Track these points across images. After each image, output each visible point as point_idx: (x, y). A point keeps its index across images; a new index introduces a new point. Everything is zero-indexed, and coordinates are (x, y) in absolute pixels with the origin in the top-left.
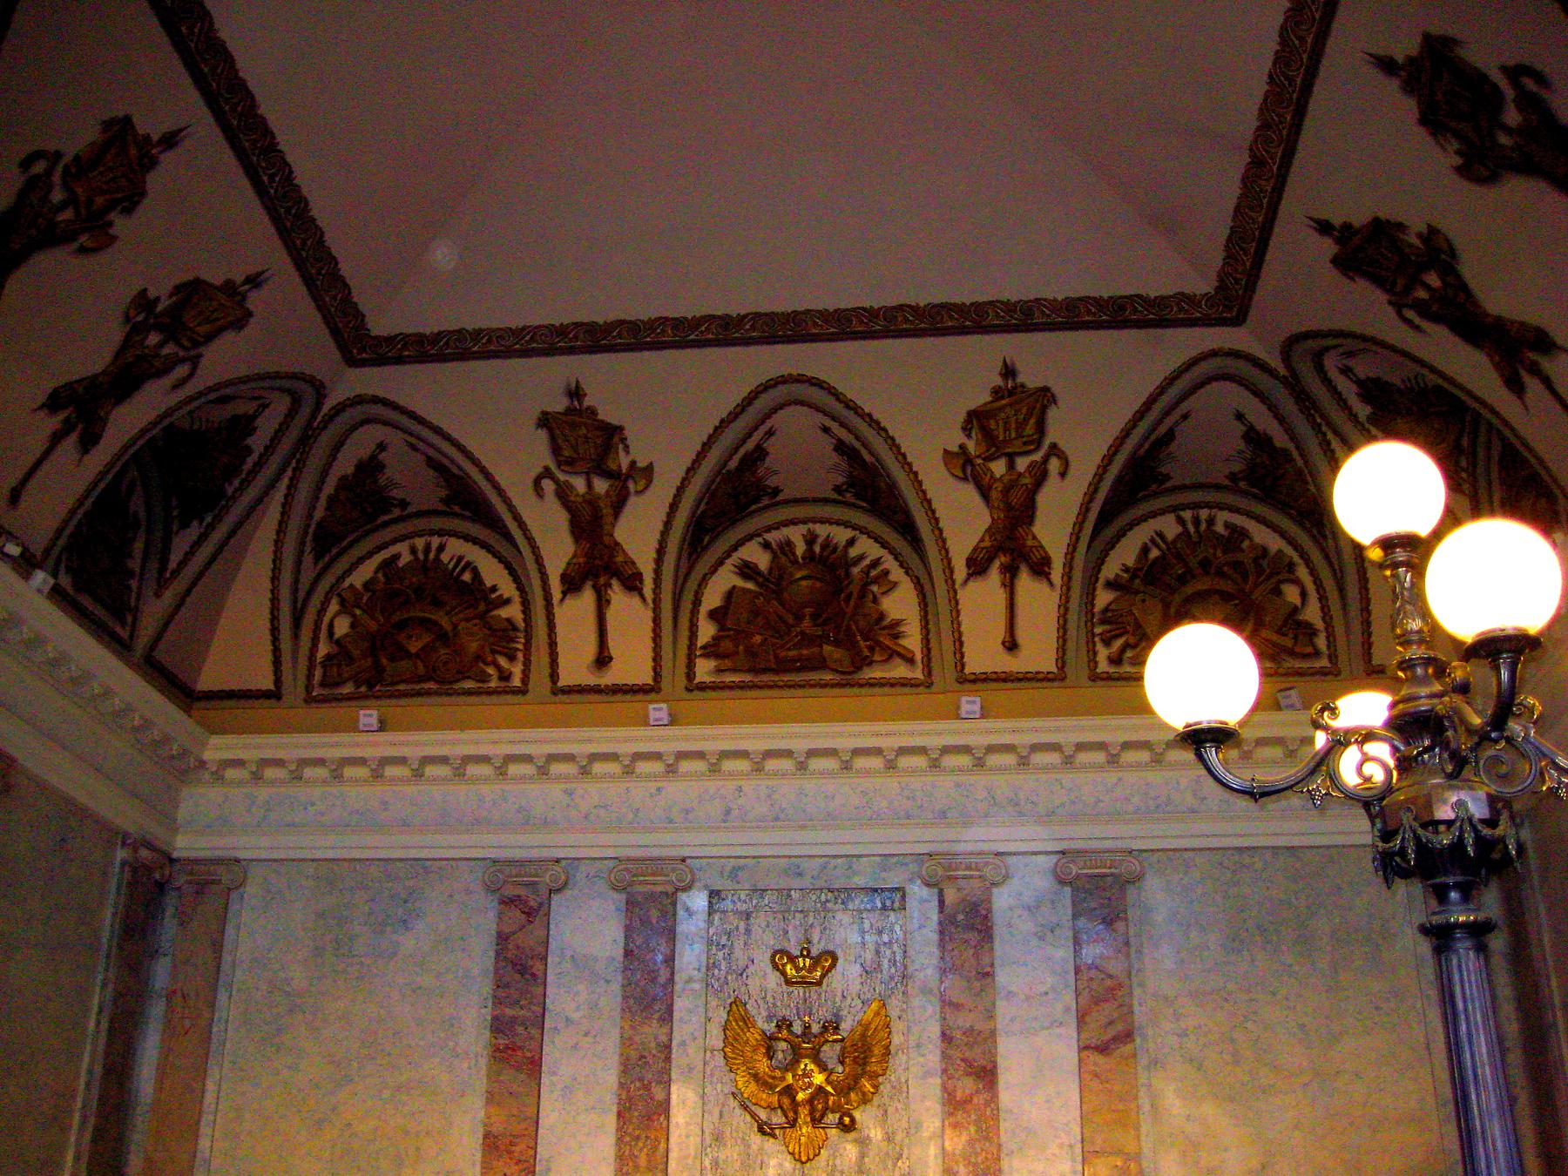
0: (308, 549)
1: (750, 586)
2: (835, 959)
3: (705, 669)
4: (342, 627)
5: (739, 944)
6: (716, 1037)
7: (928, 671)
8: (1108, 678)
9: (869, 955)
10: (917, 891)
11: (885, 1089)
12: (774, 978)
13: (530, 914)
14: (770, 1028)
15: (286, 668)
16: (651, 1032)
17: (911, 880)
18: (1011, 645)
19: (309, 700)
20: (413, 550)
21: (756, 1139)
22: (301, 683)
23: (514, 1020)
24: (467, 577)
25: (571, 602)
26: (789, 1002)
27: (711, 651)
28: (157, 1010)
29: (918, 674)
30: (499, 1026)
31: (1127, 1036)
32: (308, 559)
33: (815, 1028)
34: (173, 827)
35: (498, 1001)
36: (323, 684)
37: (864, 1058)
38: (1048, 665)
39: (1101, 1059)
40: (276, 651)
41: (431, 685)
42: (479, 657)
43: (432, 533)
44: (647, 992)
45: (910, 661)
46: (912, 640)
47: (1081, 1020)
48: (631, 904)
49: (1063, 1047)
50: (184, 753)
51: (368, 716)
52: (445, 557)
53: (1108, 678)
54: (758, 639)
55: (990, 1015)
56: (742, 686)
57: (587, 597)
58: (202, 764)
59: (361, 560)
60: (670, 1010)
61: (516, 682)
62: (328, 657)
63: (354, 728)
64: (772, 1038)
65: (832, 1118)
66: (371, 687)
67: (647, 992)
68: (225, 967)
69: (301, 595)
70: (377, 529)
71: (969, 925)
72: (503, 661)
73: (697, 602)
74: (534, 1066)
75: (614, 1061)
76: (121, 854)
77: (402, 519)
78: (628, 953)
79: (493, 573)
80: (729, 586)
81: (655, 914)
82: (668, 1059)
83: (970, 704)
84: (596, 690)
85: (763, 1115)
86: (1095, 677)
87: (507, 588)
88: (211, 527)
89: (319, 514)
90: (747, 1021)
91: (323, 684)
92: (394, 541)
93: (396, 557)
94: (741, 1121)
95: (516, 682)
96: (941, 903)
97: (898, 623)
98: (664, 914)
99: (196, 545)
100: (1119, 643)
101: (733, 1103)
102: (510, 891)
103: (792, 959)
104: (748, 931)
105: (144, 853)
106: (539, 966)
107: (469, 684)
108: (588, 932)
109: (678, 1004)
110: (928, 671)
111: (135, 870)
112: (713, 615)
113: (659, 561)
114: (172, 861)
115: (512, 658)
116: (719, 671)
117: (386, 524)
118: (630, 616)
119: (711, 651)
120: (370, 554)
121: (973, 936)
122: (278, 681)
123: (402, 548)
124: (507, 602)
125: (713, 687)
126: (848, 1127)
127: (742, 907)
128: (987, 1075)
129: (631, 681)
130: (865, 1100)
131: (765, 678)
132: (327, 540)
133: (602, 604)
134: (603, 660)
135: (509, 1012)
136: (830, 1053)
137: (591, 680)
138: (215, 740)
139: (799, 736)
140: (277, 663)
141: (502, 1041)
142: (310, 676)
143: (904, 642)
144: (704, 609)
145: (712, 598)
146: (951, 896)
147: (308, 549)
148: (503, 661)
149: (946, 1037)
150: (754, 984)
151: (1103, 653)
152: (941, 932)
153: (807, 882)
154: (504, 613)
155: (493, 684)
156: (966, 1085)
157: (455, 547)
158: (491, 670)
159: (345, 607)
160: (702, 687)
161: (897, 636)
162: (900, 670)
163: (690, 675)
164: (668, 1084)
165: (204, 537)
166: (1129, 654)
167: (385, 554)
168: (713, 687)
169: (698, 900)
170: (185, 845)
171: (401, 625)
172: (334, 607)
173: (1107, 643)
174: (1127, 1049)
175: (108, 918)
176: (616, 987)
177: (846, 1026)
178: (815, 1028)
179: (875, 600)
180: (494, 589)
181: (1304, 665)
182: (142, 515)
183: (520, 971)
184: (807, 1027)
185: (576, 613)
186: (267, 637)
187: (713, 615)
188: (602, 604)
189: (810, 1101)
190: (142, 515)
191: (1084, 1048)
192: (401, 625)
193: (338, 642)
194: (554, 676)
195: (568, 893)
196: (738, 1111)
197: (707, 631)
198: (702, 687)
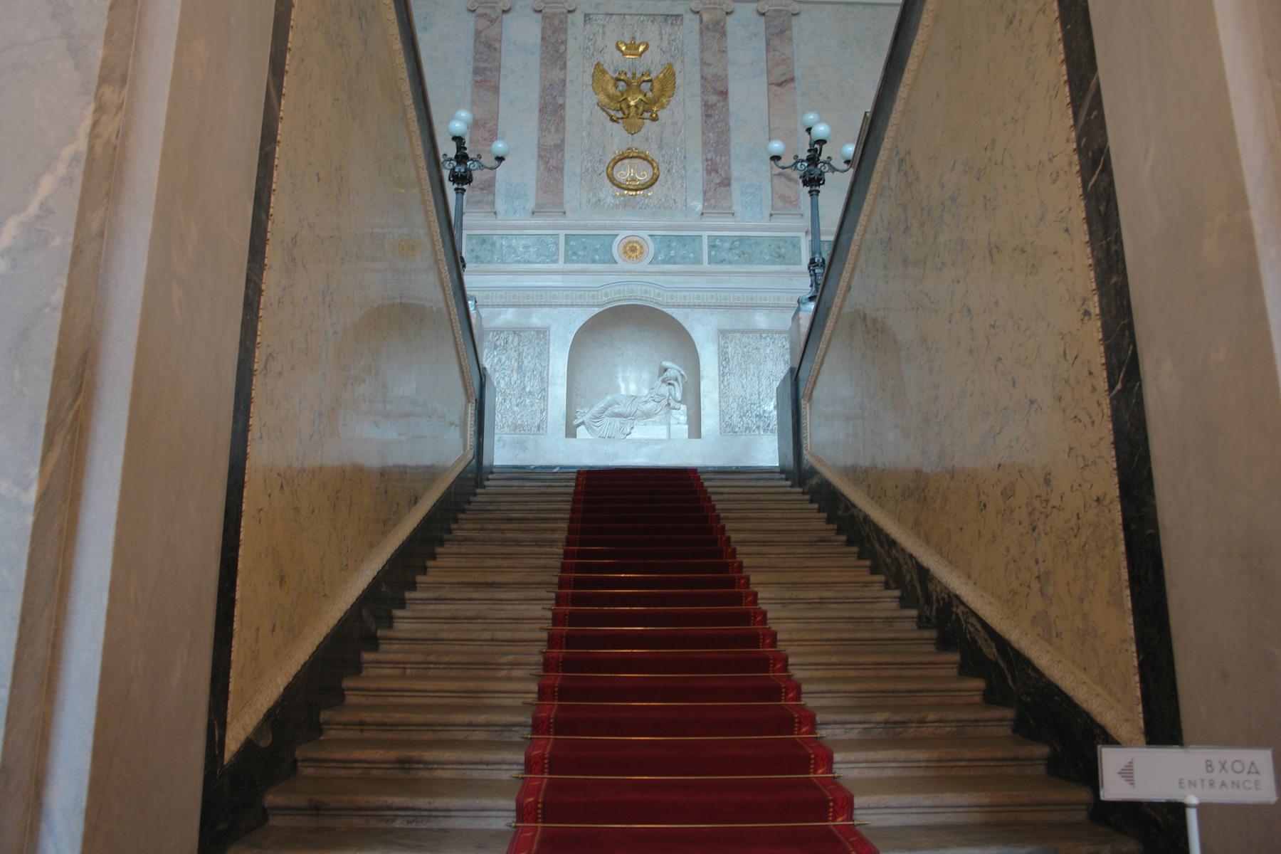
5: (599, 38)
9: (665, 44)
13: (492, 21)
16: (556, 74)
21: (610, 123)
30: (476, 71)
31: (792, 79)
35: (476, 60)
39: (779, 89)
47: (769, 72)
49: (760, 85)
55: (725, 69)
60: (565, 63)
71: (714, 30)
74: (496, 89)
78: (543, 39)
81: (556, 22)
85: (612, 113)
90: (604, 72)
96: (701, 21)
98: (561, 22)
102: (481, 11)
104: (604, 33)
106: (497, 45)
109: (569, 64)
121: (718, 35)
126: (655, 120)
128: (724, 94)
130: (663, 107)
141: (479, 78)
146: (706, 17)
149: (703, 78)
152: (701, 33)
153: (634, 11)
156: (713, 99)
164: (565, 97)
174: (790, 85)
176: (537, 57)
184: (634, 74)
189: (636, 106)
191: (770, 84)
196: (600, 112)
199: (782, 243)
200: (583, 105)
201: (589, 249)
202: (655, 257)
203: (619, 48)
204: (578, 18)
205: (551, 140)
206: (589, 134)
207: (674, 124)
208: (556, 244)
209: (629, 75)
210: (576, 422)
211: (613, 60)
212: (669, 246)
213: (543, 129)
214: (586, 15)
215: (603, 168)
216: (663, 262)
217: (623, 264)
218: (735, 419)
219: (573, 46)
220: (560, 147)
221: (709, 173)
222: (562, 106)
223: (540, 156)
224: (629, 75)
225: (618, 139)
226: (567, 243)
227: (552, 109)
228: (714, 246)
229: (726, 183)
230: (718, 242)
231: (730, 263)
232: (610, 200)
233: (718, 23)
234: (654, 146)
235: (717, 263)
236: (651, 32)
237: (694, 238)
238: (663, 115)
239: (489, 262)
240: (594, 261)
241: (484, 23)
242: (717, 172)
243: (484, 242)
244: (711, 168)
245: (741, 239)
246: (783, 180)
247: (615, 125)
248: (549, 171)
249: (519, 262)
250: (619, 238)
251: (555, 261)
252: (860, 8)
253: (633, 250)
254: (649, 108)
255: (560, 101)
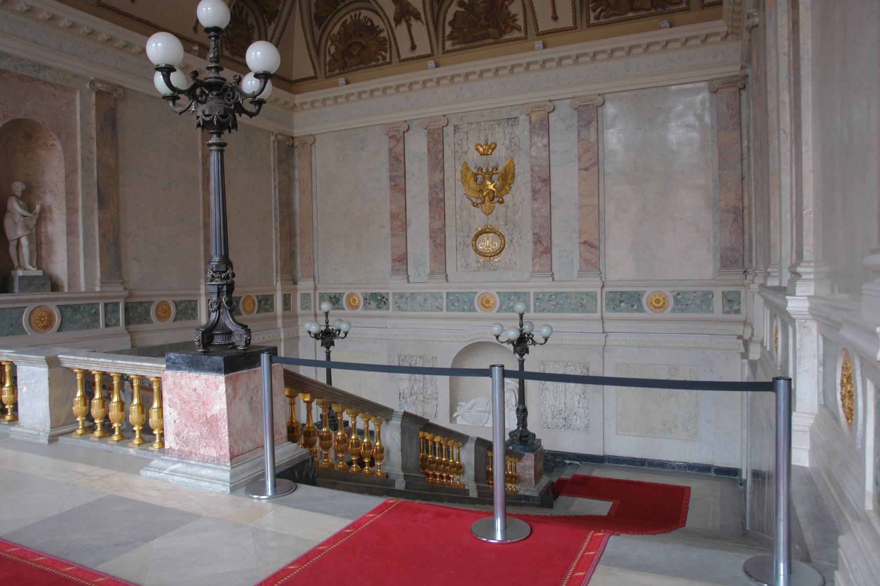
0: (314, 24)
1: (462, 10)
2: (496, 145)
3: (448, 44)
4: (333, 50)
5: (464, 143)
6: (459, 176)
7: (526, 33)
8: (594, 25)
9: (507, 142)
10: (523, 118)
11: (513, 188)
12: (477, 154)
13: (398, 140)
14: (475, 171)
15: (317, 67)
16: (438, 176)
17: (521, 114)
18: (555, 18)
19: (326, 77)
20: (351, 17)
21: (473, 208)
22: (323, 71)
23: (396, 176)
24: (369, 24)
25: (398, 27)
26: (481, 161)
27: (451, 37)
28: (297, 185)
29: (522, 35)
30: (392, 179)
32: (316, 28)
33: (490, 170)
34: (292, 127)
35: (391, 171)
36: (330, 71)
37: (507, 178)
38: (570, 24)
40: (313, 62)
41: (362, 66)
42: (376, 53)
43: (356, 9)
44: (436, 161)
45: (520, 30)
46: (520, 22)
47: (579, 160)
48: (429, 133)
50: (286, 103)
51: (342, 80)
52: (361, 18)
53: (594, 25)
54: (466, 30)
56: (465, 49)
57: (404, 25)
58: (295, 106)
59: (336, 24)
60: (443, 168)
61: (388, 60)
62: (330, 61)
63: (337, 85)
64: (476, 174)
65: (496, 199)
66: (343, 69)
67: (436, 161)
68: (313, 167)
69: (317, 41)
70: (338, 12)
71: (542, 127)
72: (383, 53)
73: (444, 19)
74: (404, 191)
75: (427, 188)
76: (272, 138)
77: (345, 6)
78: (429, 150)
79: (377, 21)
80: (454, 11)
81: (436, 136)
82: (444, 184)
83: (538, 44)
84: (413, 59)
85: (474, 200)
86: (589, 26)
87: (382, 26)
88: (277, 24)
89: (313, 10)
90: (468, 169)
91: (330, 71)
92: (344, 15)
93: (346, 20)
94: (468, 202)
95: (388, 60)
97: (515, 15)
99: (275, 31)
100: (598, 11)
101: (465, 197)
102: (391, 134)
103: (482, 146)
105: (280, 137)
107: (374, 63)
108: (417, 145)
110: (526, 33)
111: (278, 143)
112: (451, 23)
113: (424, 6)
114: (293, 138)
115: (386, 51)
116: (453, 44)
117: (340, 9)
118: (419, 29)
119: (451, 37)
120: (338, 21)
122: (315, 73)
123: (348, 17)
124: (382, 31)
125: (452, 51)
126: (502, 202)
127: (465, 130)
128: (547, 181)
129: (423, 53)
131: (469, 45)
132: (321, 20)
133: (409, 27)
134: (413, 47)
135: (394, 174)
136: (495, 177)
137: (411, 55)
138: (297, 96)
139: (476, 66)
140: (314, 66)
142: (325, 69)
143: (517, 23)
144: (447, 22)
145: (450, 17)
146: (533, 118)
147: (314, 24)
148: (383, 53)
150: (470, 156)
151: (592, 15)
154: (382, 35)
155: (381, 62)
156: (539, 185)
157: (365, 13)
158: (380, 57)
159: (333, 43)
160: (448, 52)
161: (515, 21)
162: (516, 34)
163: (444, 48)
165: (276, 27)
166: (603, 14)
167: (343, 20)
168: (452, 51)
169: (450, 129)
170: (297, 132)
171: (350, 46)
172: (329, 43)
173: (594, 11)
175: (272, 160)
177: (501, 168)
178: (490, 170)
179: (507, 8)
180: (378, 26)
181: (676, 8)
182: (255, 24)
183: (398, 161)
184: (487, 170)
185: (401, 31)
186: (309, 58)
187: (451, 23)
188: (409, 27)
189: (488, 194)
190: (255, 24)
191: (580, 169)
192: (350, 46)
193: (332, 56)
194: (399, 56)
195: (410, 132)
197: (448, 30)
198: (448, 52)
199: (584, 296)
200: (456, 196)
201: (461, 302)
202: (501, 306)
203: (477, 150)
204: (450, 129)
205: (437, 224)
206: (460, 217)
207: (514, 205)
208: (441, 297)
209: (484, 170)
210: (455, 415)
211: (474, 159)
212: (509, 299)
213: (432, 218)
214: (455, 126)
215: (469, 241)
216: (506, 310)
217: (480, 312)
218: (549, 420)
219: (448, 152)
220: (443, 229)
221: (535, 243)
222: (443, 200)
223: (431, 237)
224: (484, 170)
225: (479, 219)
226: (447, 297)
227: (437, 204)
228: (538, 299)
229: (548, 251)
230: (541, 296)
231: (549, 311)
232: (474, 265)
233: (542, 121)
234: (502, 223)
235: (540, 311)
236: (499, 136)
237: (525, 294)
238: (507, 198)
239: (405, 310)
240: (464, 310)
241: (394, 142)
242: (541, 243)
243: (402, 297)
244: (537, 240)
245: (557, 294)
246: (587, 247)
247: (477, 209)
248: (437, 247)
249: (421, 310)
250: (477, 296)
251: (441, 310)
252: (654, 89)
253: (488, 301)
254: (497, 197)
255: (441, 196)
